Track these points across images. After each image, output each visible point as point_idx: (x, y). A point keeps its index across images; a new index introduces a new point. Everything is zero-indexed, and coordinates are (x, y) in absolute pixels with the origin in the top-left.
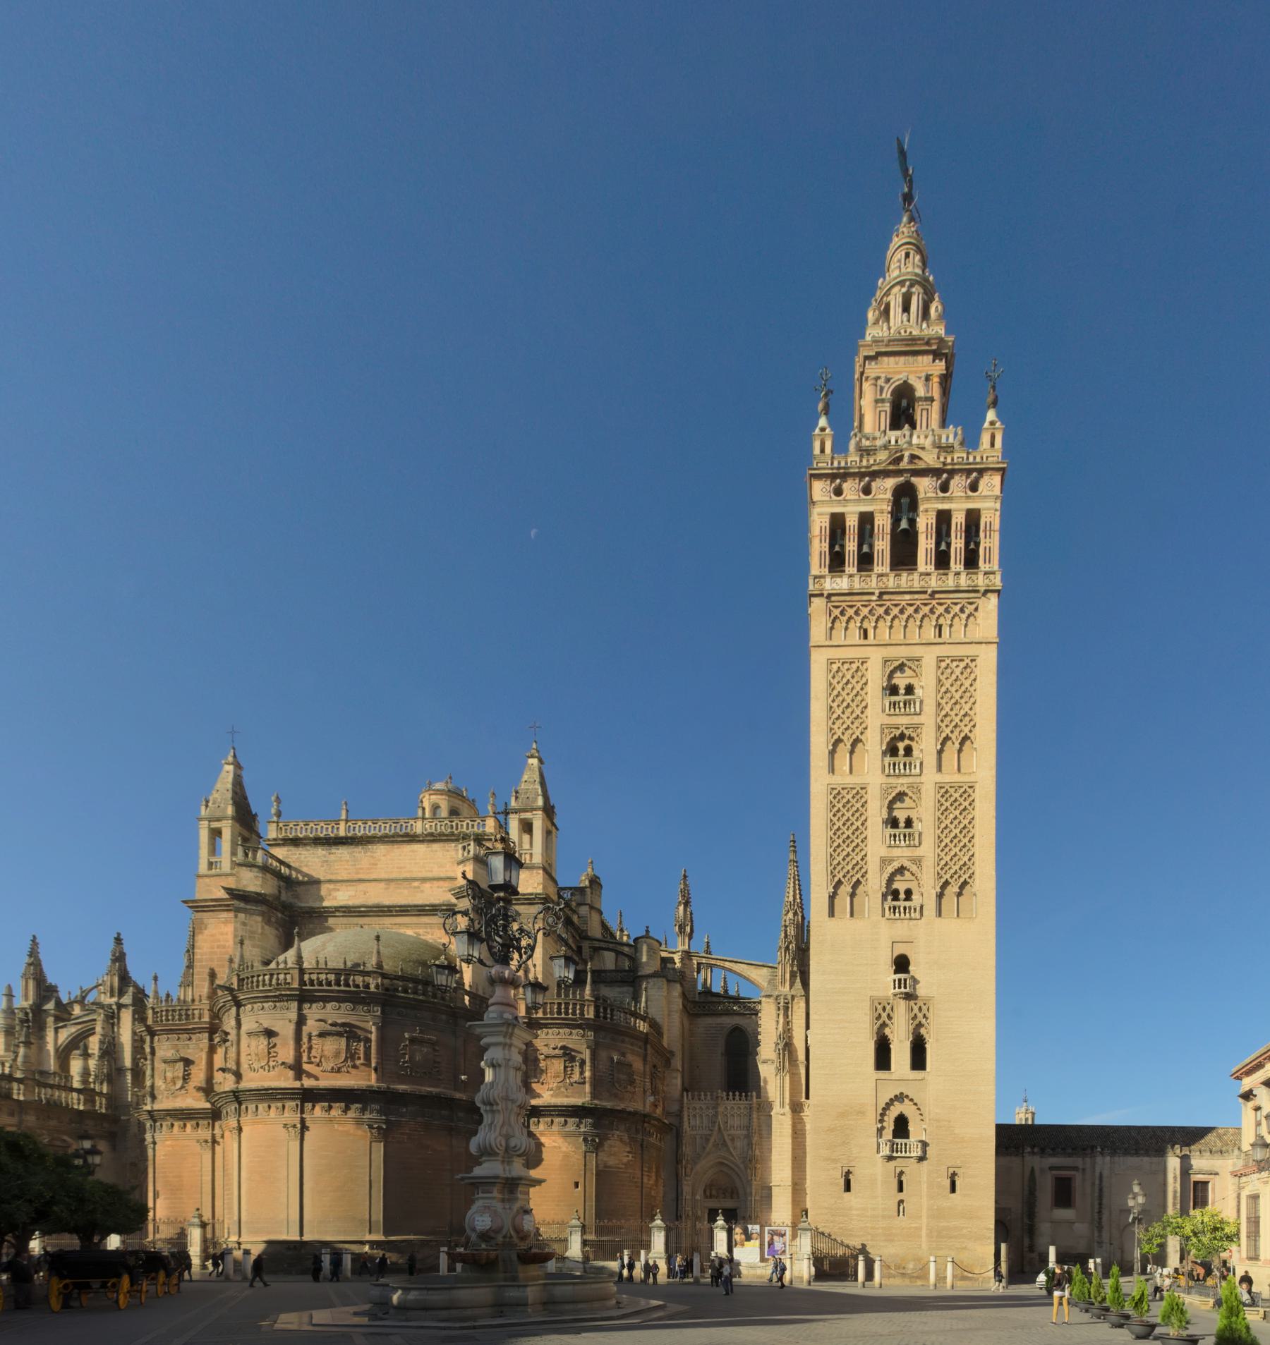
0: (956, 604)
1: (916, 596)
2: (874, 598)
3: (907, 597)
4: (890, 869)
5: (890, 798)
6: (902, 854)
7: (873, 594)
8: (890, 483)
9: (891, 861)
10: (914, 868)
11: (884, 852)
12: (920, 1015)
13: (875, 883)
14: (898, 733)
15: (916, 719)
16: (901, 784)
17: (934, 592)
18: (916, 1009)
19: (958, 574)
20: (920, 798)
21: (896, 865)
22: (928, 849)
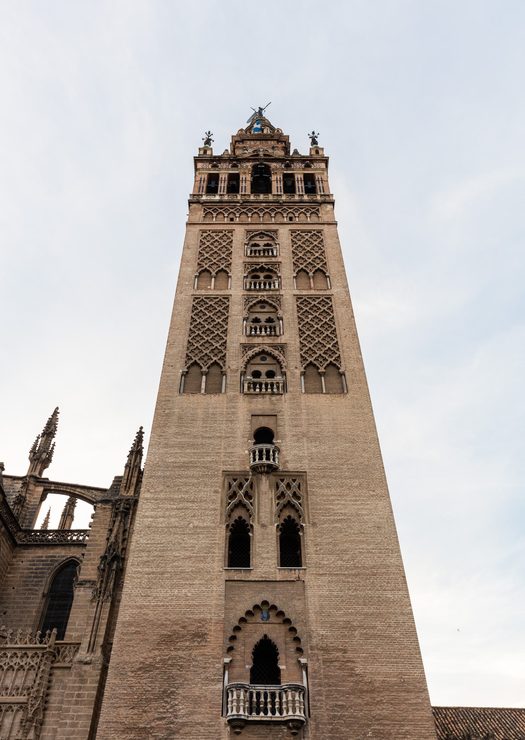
0: (302, 208)
1: (270, 204)
2: (239, 205)
3: (264, 204)
4: (250, 353)
5: (251, 304)
6: (263, 341)
7: (238, 202)
8: (249, 165)
9: (251, 346)
10: (276, 353)
11: (243, 340)
12: (289, 493)
13: (235, 361)
14: (258, 267)
15: (273, 260)
16: (263, 295)
17: (284, 202)
18: (283, 485)
19: (302, 195)
20: (280, 305)
21: (257, 350)
22: (289, 335)
